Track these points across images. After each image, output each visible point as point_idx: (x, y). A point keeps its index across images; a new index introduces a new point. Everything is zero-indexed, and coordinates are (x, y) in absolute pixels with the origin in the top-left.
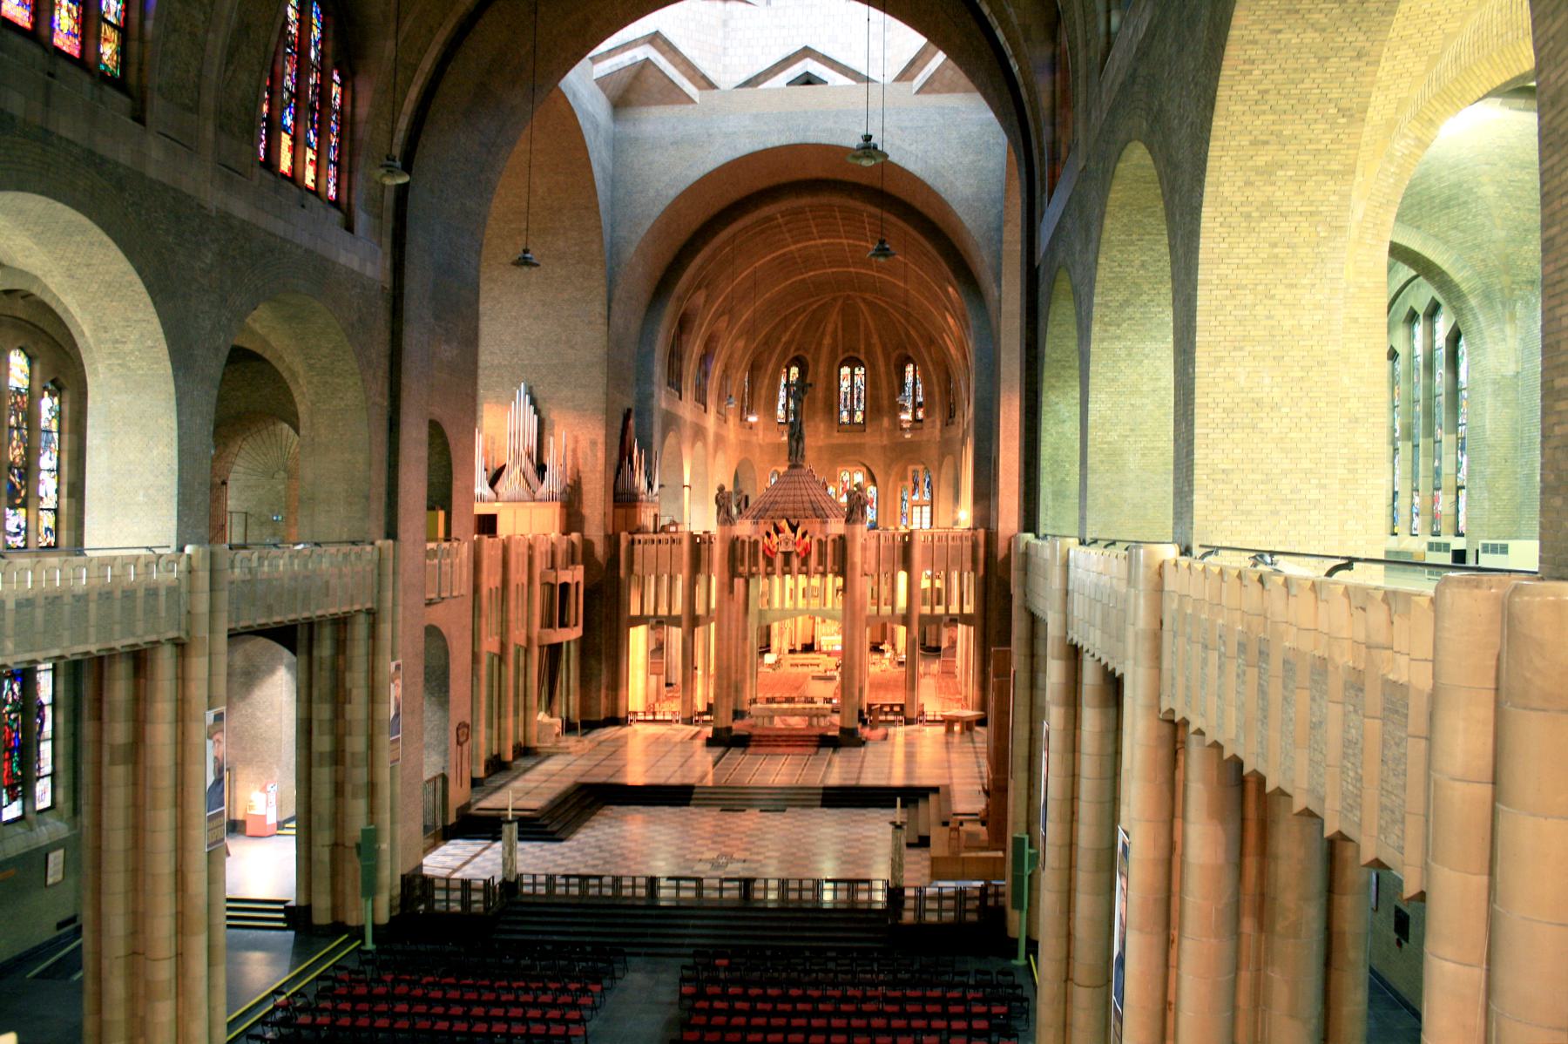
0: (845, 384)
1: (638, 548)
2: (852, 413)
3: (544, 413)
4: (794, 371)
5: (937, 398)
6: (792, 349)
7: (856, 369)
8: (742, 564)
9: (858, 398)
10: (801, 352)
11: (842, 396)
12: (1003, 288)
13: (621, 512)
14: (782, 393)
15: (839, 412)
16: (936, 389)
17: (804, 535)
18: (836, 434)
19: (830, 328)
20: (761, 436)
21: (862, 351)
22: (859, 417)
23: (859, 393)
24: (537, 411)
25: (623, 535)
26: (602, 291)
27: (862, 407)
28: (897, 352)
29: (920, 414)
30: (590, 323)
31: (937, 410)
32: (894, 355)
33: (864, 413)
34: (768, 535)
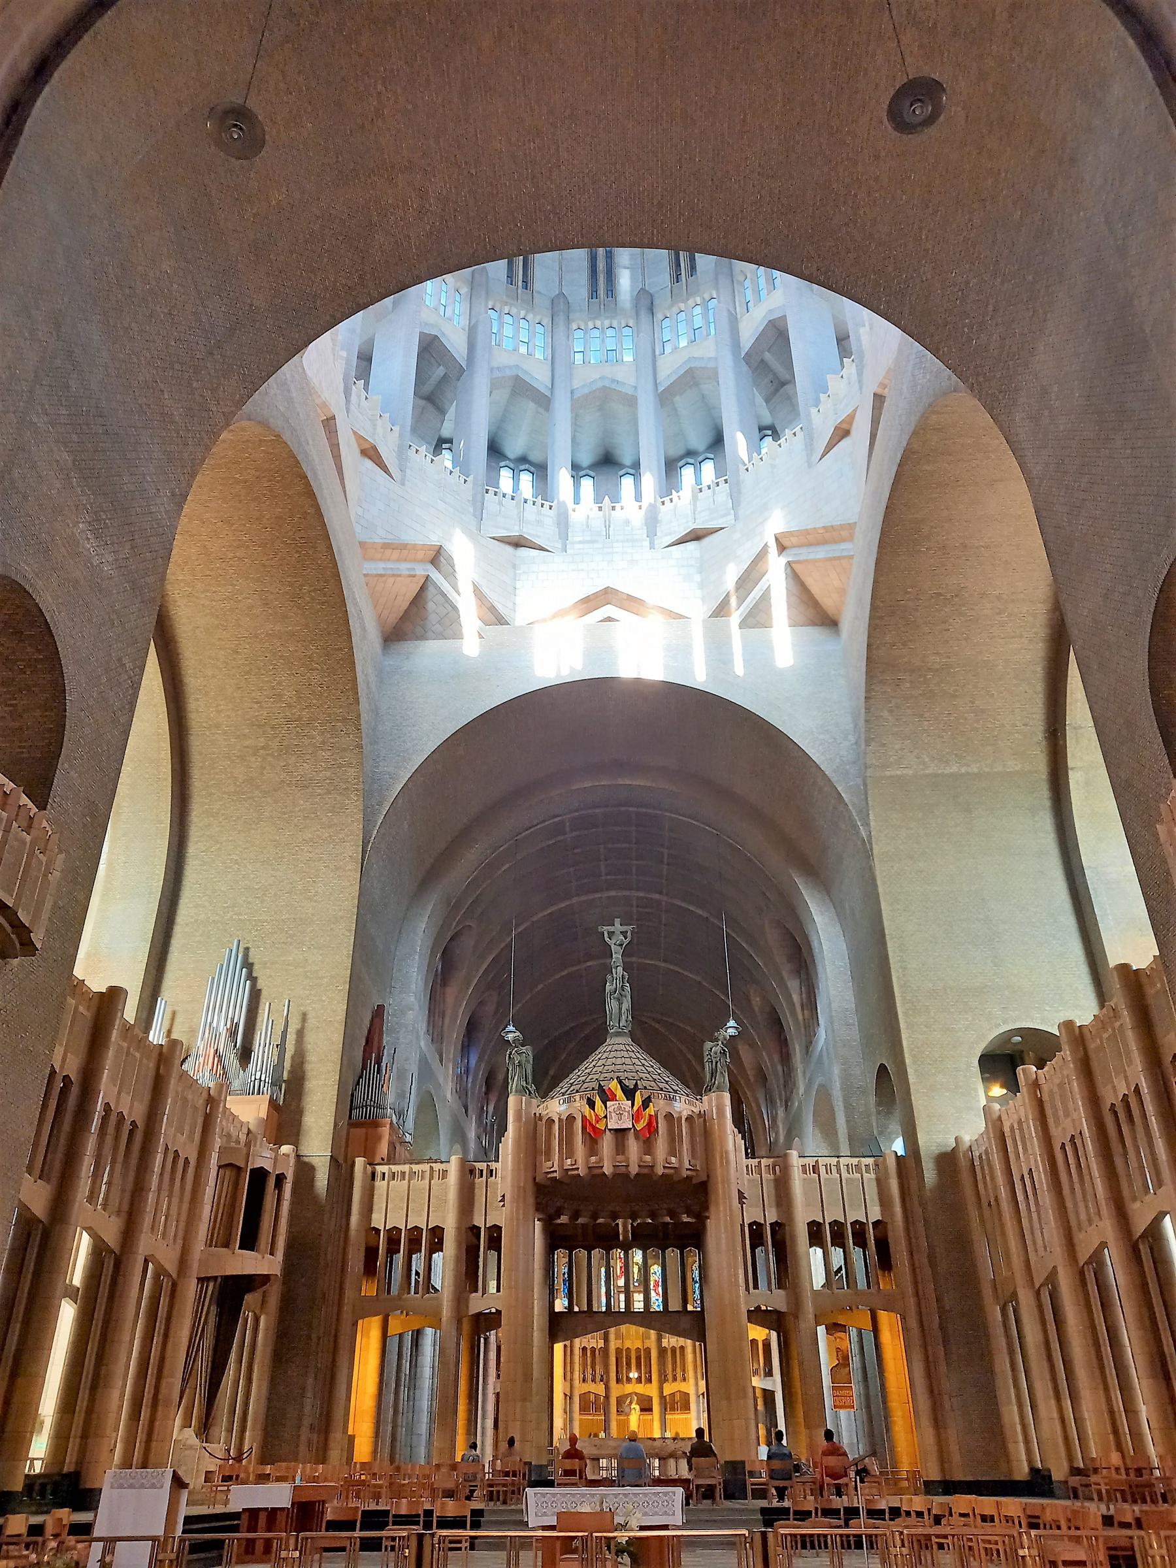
1: (380, 1185)
3: (261, 984)
8: (548, 1157)
12: (872, 824)
13: (359, 1132)
17: (646, 1103)
24: (251, 978)
25: (360, 1162)
26: (358, 828)
30: (337, 868)
34: (591, 1104)
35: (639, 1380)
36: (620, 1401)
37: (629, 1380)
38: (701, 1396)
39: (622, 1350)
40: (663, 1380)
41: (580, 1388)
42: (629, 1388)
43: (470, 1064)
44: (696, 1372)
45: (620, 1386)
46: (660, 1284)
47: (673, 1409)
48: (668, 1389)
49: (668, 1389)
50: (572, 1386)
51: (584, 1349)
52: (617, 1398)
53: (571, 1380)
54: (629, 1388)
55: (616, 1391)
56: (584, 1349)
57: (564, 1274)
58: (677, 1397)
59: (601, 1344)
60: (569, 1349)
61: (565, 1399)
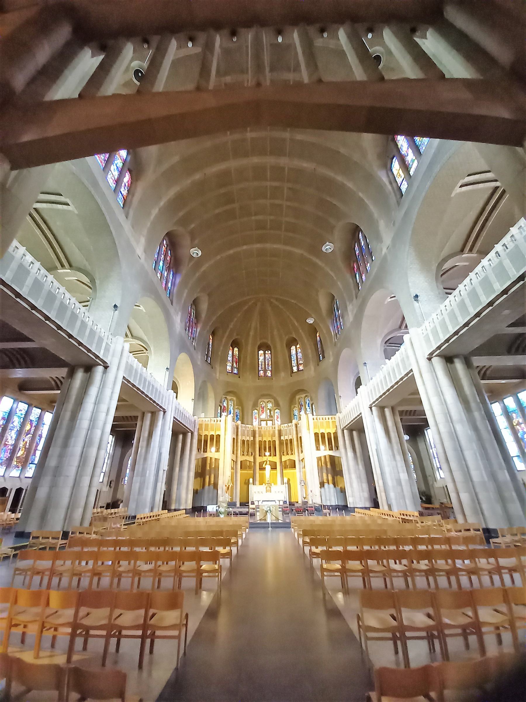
0: (261, 358)
2: (265, 371)
4: (236, 349)
5: (310, 356)
6: (235, 334)
7: (266, 351)
9: (268, 364)
10: (239, 337)
11: (260, 363)
14: (230, 358)
15: (259, 371)
16: (310, 351)
18: (258, 381)
19: (253, 325)
20: (218, 375)
21: (269, 338)
22: (269, 374)
23: (268, 362)
27: (270, 368)
28: (287, 337)
29: (301, 368)
31: (311, 361)
32: (285, 338)
33: (271, 371)
35: (270, 455)
36: (261, 464)
37: (265, 456)
38: (301, 461)
39: (262, 441)
40: (282, 454)
41: (240, 458)
42: (265, 459)
43: (176, 282)
44: (298, 450)
45: (261, 457)
46: (279, 417)
47: (286, 468)
48: (284, 458)
49: (284, 458)
50: (237, 457)
51: (244, 441)
52: (259, 463)
53: (237, 454)
54: (265, 459)
55: (259, 460)
56: (244, 441)
57: (237, 412)
58: (288, 463)
59: (252, 438)
60: (235, 440)
61: (234, 463)
